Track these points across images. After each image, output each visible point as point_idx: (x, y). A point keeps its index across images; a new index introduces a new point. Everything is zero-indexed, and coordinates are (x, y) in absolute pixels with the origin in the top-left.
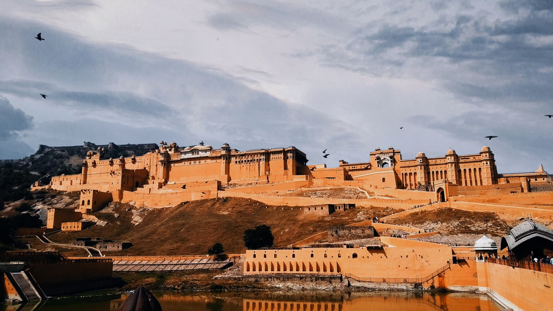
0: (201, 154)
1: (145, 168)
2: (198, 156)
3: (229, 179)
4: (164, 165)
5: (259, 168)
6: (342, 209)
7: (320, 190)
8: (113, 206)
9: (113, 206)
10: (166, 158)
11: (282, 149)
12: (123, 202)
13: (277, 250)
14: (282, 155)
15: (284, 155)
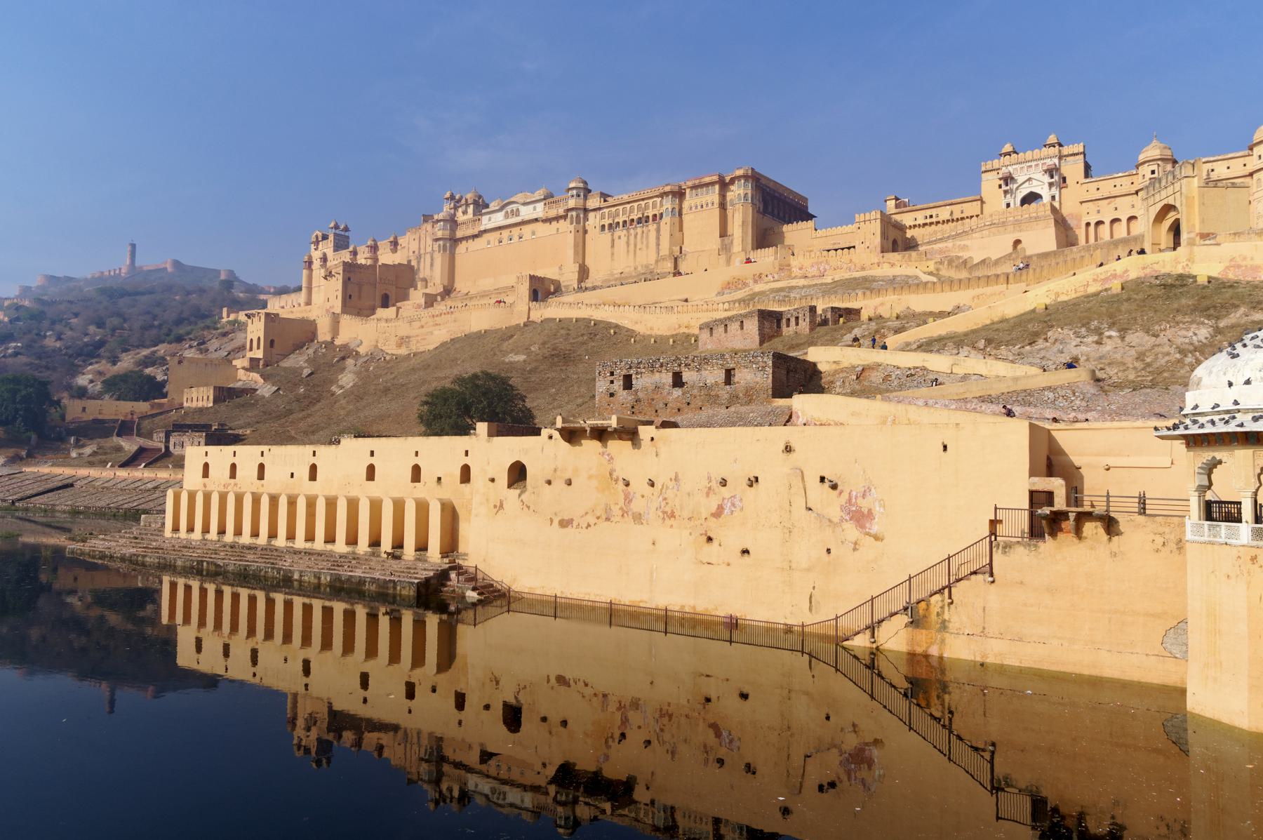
0: (527, 212)
1: (409, 261)
2: (518, 219)
3: (584, 272)
4: (445, 250)
5: (658, 238)
6: (804, 326)
7: (804, 287)
8: (311, 351)
9: (311, 351)
10: (447, 232)
11: (715, 178)
12: (338, 342)
13: (265, 448)
14: (713, 195)
15: (723, 196)
